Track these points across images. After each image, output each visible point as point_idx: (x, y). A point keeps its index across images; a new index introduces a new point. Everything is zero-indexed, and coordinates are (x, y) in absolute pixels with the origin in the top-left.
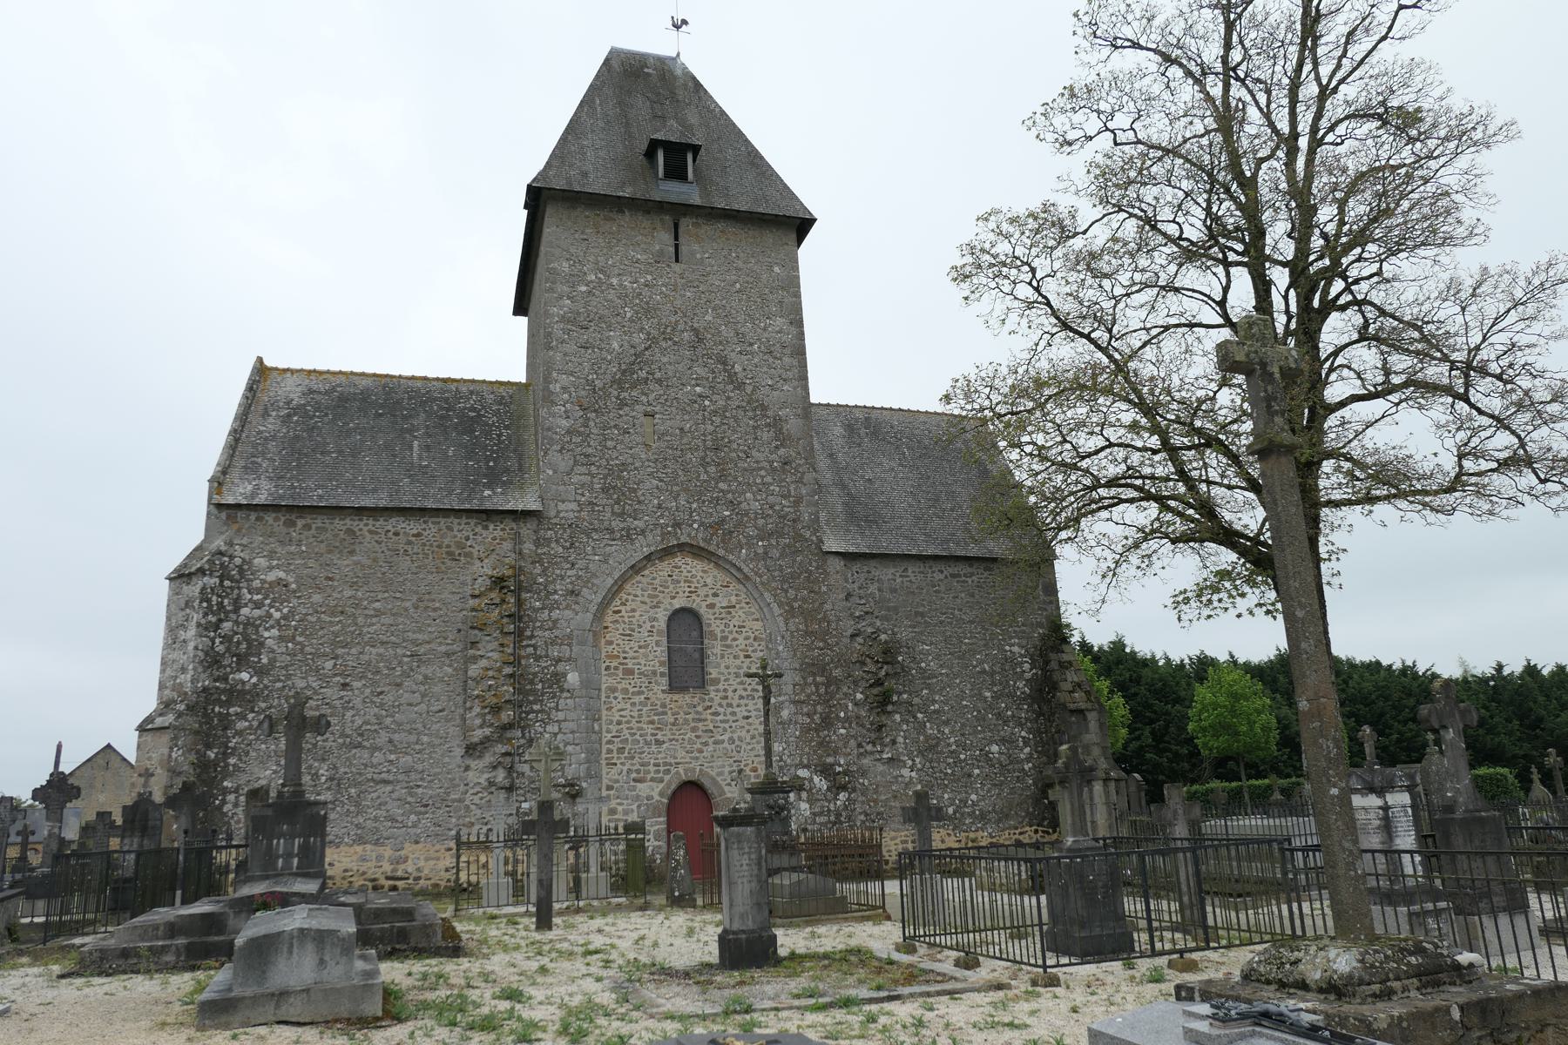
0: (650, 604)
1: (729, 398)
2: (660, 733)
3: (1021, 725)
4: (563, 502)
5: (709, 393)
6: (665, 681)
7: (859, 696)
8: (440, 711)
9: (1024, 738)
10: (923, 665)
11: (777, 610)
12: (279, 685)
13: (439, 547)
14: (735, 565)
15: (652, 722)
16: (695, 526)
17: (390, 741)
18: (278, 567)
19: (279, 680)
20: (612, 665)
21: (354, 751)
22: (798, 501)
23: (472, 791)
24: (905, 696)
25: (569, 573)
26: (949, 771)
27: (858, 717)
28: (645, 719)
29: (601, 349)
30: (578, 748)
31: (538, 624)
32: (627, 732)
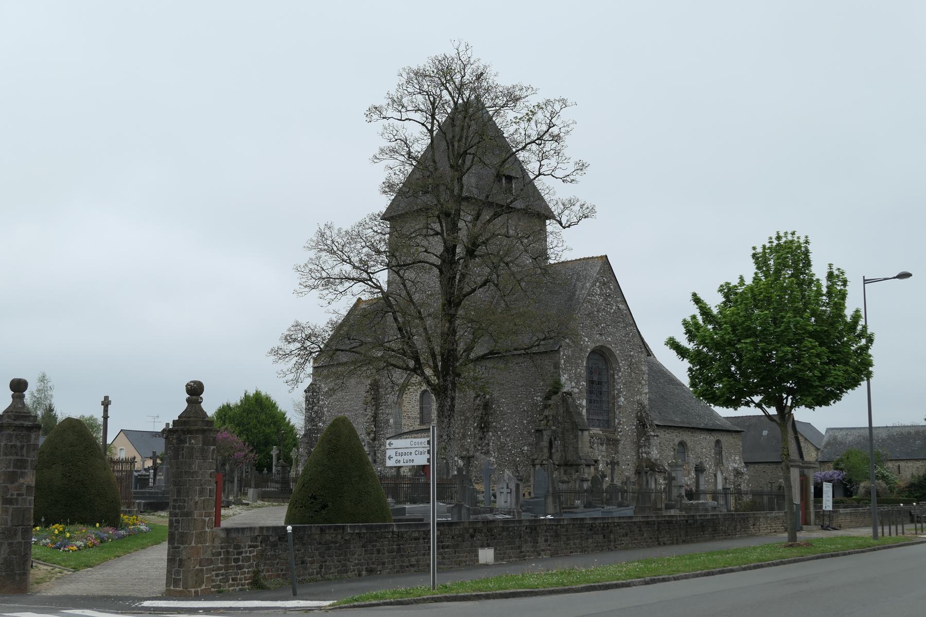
6: (418, 420)
10: (502, 409)
24: (494, 424)
26: (507, 459)
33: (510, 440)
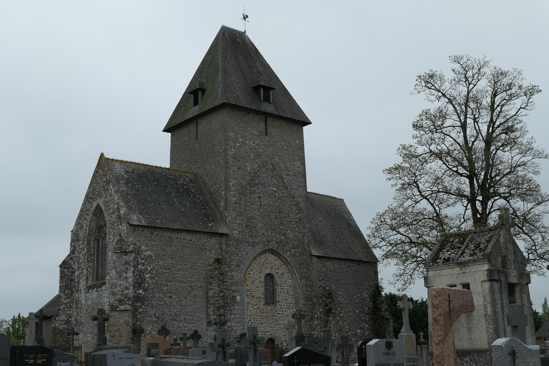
0: (259, 271)
1: (283, 193)
2: (262, 320)
3: (366, 323)
4: (234, 230)
5: (277, 190)
6: (263, 300)
7: (321, 310)
8: (199, 308)
9: (367, 328)
10: (339, 299)
11: (298, 277)
12: (151, 295)
13: (197, 245)
14: (285, 258)
15: (260, 316)
16: (274, 242)
17: (185, 319)
18: (149, 250)
19: (151, 294)
20: (248, 294)
21: (174, 322)
22: (303, 235)
23: (209, 339)
25: (237, 258)
27: (320, 317)
28: (258, 315)
29: (244, 170)
30: (240, 324)
31: (228, 277)
32: (252, 319)
33: (346, 324)
